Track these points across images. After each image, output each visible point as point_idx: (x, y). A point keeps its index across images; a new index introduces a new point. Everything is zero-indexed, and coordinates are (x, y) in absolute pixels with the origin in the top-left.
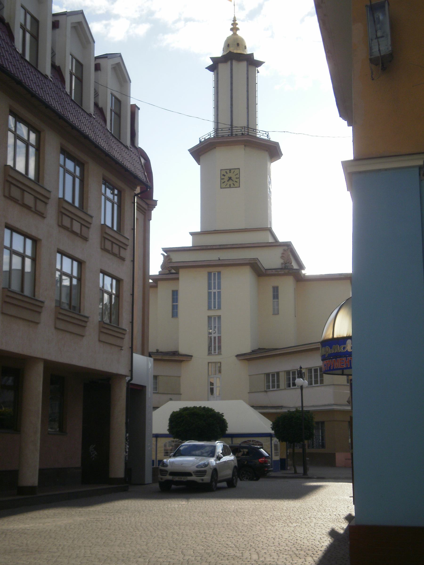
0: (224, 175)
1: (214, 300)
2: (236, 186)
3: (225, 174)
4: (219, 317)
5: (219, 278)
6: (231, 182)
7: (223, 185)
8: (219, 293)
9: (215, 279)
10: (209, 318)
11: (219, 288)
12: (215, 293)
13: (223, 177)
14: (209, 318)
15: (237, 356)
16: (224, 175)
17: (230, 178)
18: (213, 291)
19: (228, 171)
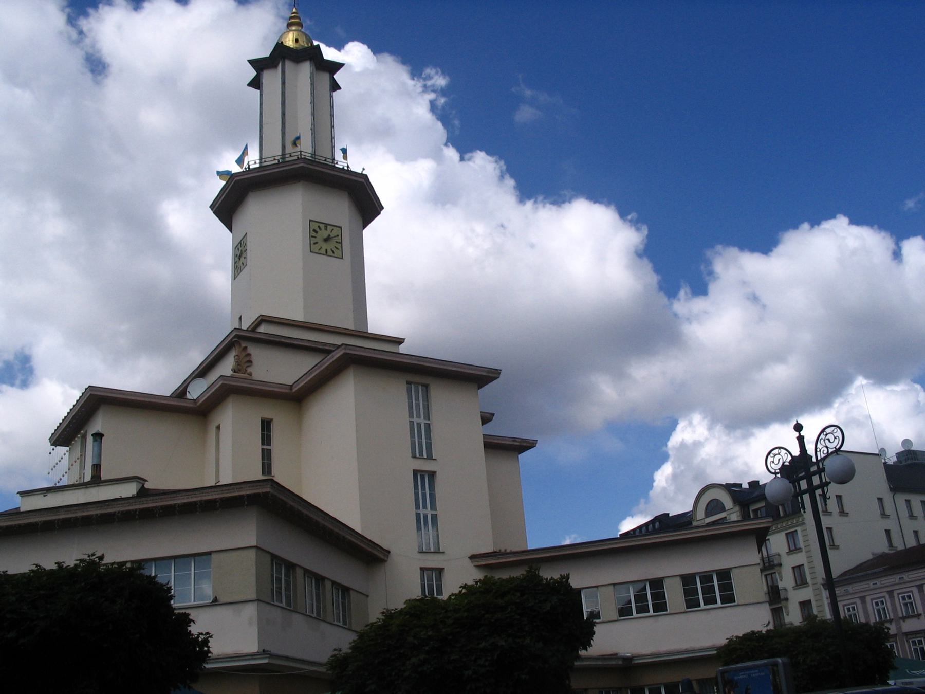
0: (314, 230)
1: (422, 442)
2: (336, 255)
3: (318, 229)
4: (432, 475)
5: (427, 399)
6: (325, 246)
7: (314, 247)
8: (428, 426)
9: (417, 399)
10: (415, 472)
11: (427, 416)
12: (419, 425)
13: (313, 234)
14: (415, 472)
15: (473, 557)
16: (314, 230)
17: (326, 240)
18: (416, 420)
19: (322, 226)
